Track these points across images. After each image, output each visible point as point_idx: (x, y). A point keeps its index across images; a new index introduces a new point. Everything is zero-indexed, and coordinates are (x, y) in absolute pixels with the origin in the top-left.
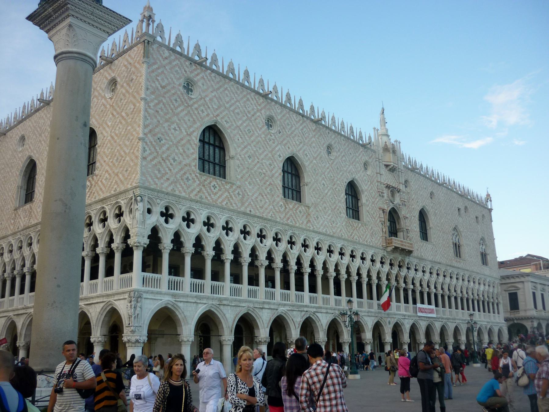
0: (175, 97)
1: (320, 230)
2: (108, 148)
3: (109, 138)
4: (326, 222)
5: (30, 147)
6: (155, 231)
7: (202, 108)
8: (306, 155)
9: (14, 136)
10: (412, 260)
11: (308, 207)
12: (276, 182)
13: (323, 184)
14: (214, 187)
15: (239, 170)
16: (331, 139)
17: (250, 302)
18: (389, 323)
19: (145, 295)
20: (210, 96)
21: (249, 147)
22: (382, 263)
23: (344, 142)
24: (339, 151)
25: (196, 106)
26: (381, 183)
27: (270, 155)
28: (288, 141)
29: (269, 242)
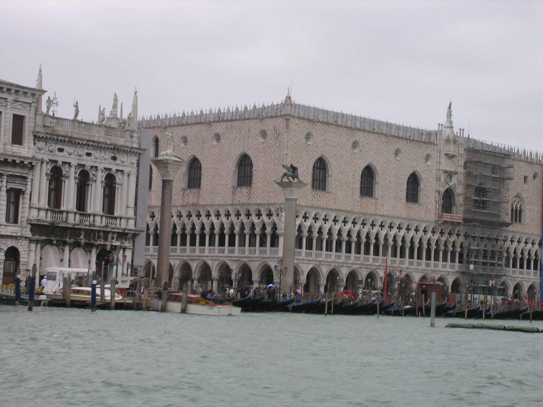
1: (384, 214)
2: (262, 174)
3: (262, 168)
4: (389, 208)
5: (193, 149)
7: (315, 149)
8: (379, 162)
9: (175, 133)
11: (377, 199)
13: (390, 181)
15: (334, 183)
16: (399, 144)
17: (336, 262)
22: (433, 232)
25: (311, 149)
26: (439, 170)
27: (353, 169)
28: (367, 156)
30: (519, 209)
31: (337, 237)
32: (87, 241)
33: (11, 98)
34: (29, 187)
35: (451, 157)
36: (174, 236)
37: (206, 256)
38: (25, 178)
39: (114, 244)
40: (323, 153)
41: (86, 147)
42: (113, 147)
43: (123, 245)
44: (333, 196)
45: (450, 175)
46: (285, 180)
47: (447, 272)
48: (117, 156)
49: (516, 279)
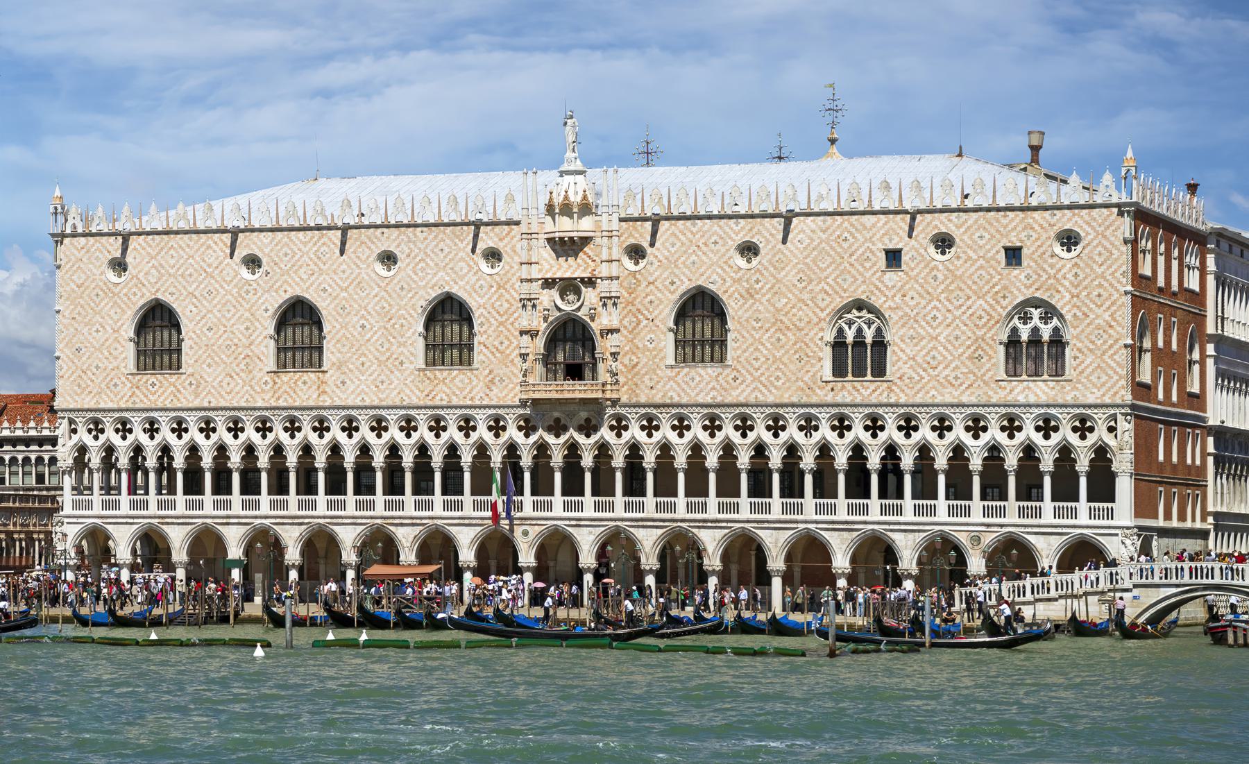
0: (97, 290)
1: (350, 403)
6: (82, 450)
8: (325, 290)
12: (256, 351)
13: (363, 327)
14: (153, 385)
15: (191, 353)
18: (525, 533)
19: (66, 520)
21: (209, 315)
23: (421, 236)
24: (408, 256)
25: (125, 290)
27: (247, 314)
28: (286, 282)
30: (869, 340)
40: (160, 297)
44: (191, 379)
45: (569, 287)
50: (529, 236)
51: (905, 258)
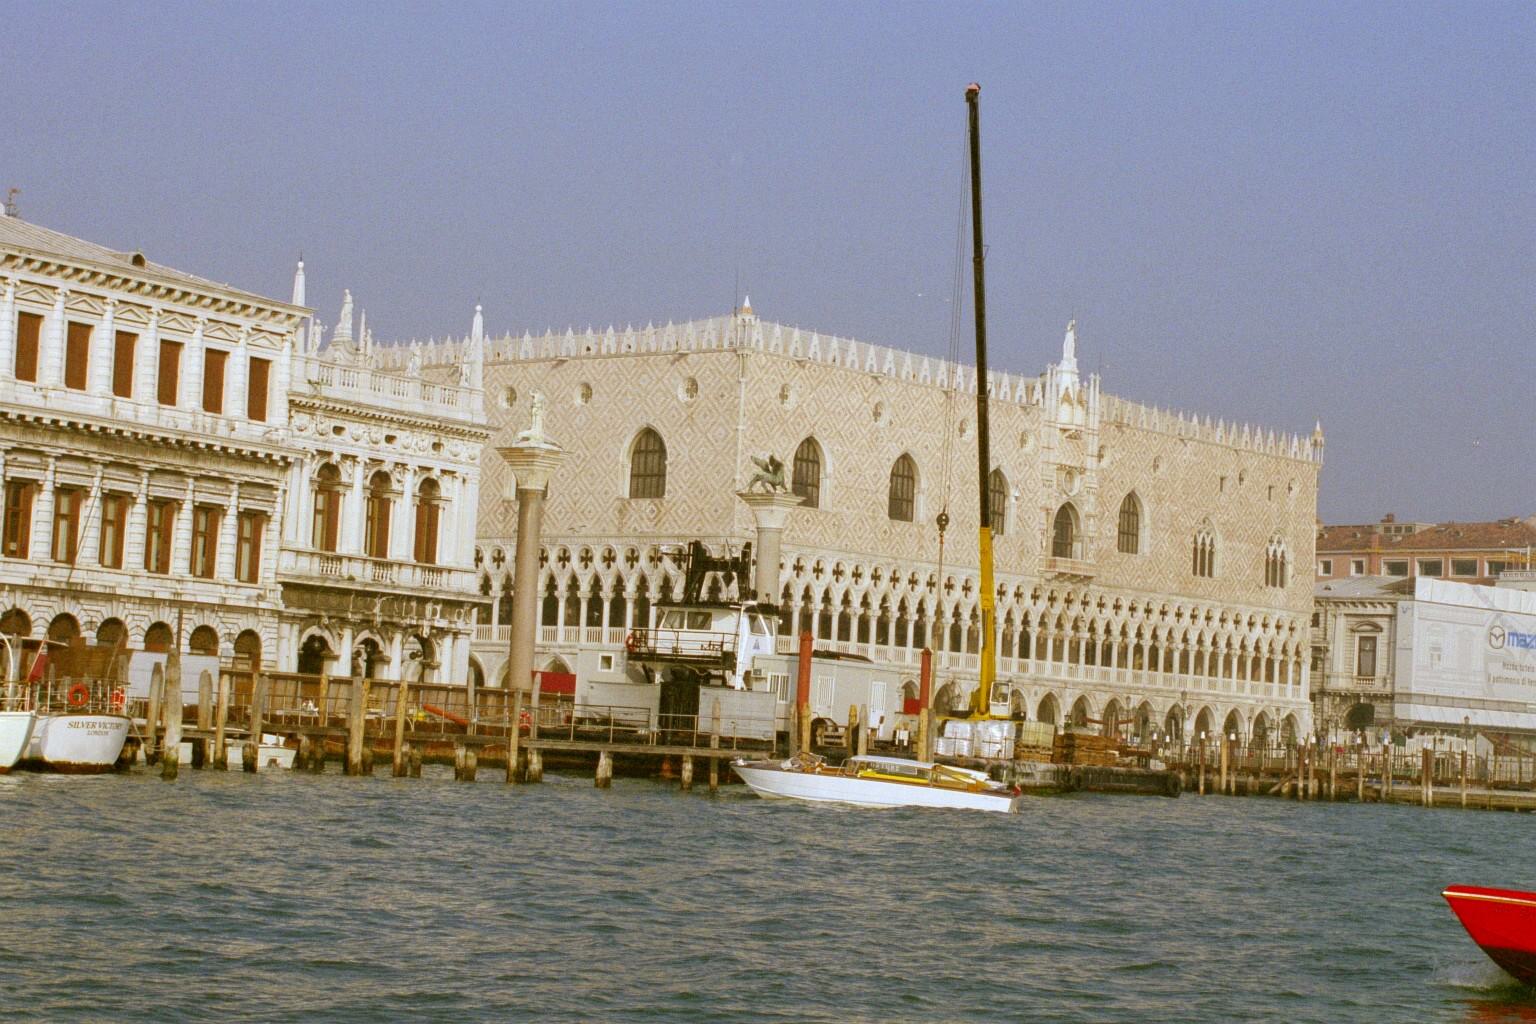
3: (687, 459)
8: (927, 447)
10: (1094, 592)
11: (923, 527)
14: (808, 521)
18: (1036, 694)
20: (808, 401)
22: (1035, 597)
27: (876, 461)
29: (866, 581)
31: (802, 604)
32: (387, 619)
33: (247, 324)
34: (278, 507)
35: (1075, 437)
36: (550, 606)
37: (560, 647)
38: (270, 487)
39: (436, 624)
41: (385, 424)
42: (437, 424)
43: (453, 626)
45: (1070, 472)
46: (758, 488)
47: (1062, 682)
48: (443, 441)
49: (1203, 697)
50: (1049, 424)
51: (1227, 484)
